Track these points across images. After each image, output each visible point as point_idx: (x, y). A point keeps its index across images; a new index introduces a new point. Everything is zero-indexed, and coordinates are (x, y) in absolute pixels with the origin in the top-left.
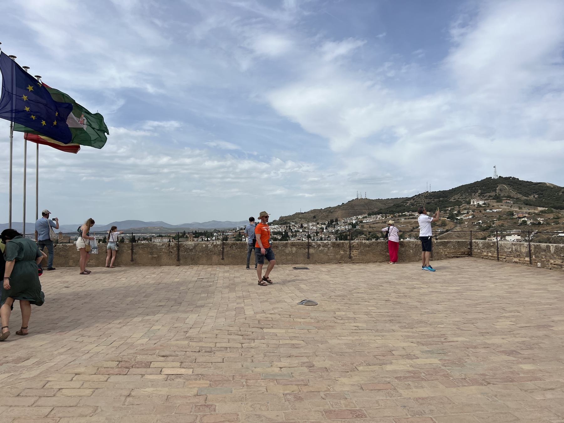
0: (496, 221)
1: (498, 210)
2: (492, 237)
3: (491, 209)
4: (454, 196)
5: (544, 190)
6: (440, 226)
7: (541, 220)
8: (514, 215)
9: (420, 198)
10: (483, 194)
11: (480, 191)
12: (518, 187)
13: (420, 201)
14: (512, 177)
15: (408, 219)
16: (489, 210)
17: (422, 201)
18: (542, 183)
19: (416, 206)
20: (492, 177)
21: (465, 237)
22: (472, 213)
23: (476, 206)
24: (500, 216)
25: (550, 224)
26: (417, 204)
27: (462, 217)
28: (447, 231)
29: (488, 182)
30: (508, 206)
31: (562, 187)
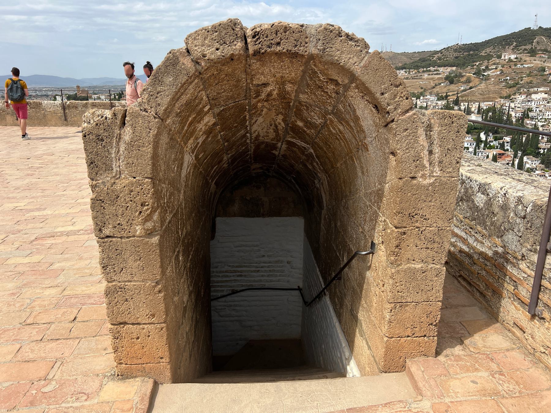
0: (525, 77)
2: (517, 94)
3: (522, 65)
11: (515, 43)
15: (432, 75)
19: (444, 60)
23: (507, 61)
27: (489, 73)
28: (471, 88)
30: (541, 61)
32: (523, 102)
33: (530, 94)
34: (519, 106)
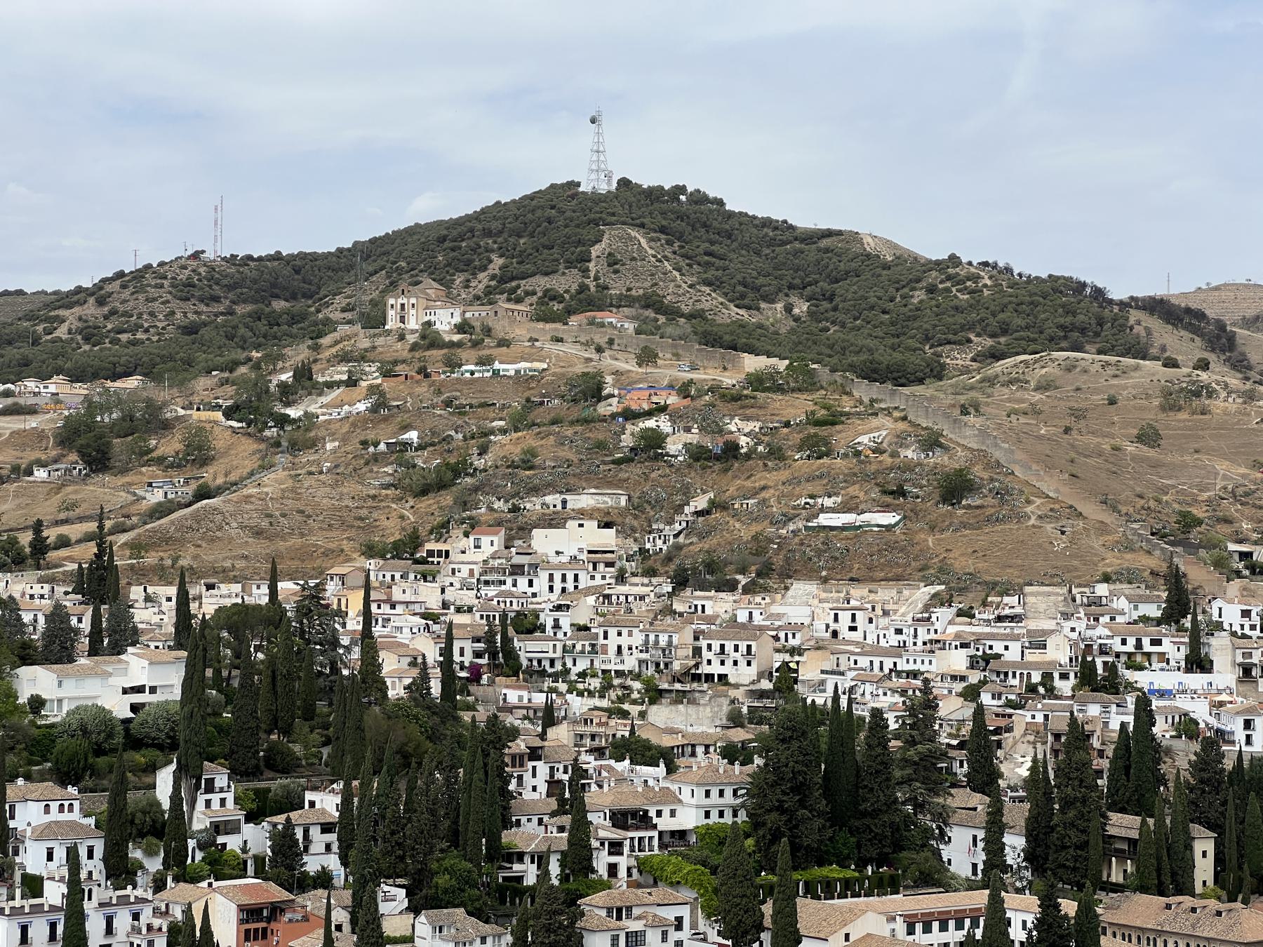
0: (504, 431)
1: (528, 365)
3: (484, 362)
4: (348, 291)
5: (847, 273)
6: (172, 466)
7: (741, 429)
8: (600, 398)
9: (140, 289)
10: (514, 284)
11: (498, 262)
12: (715, 248)
13: (140, 316)
14: (690, 189)
16: (472, 367)
17: (152, 314)
18: (839, 233)
19: (115, 342)
20: (578, 184)
21: (302, 535)
22: (379, 381)
24: (528, 400)
25: (782, 458)
26: (119, 333)
27: (313, 409)
28: (203, 493)
29: (553, 207)
31: (930, 261)
32: (487, 576)
33: (524, 531)
34: (468, 598)
